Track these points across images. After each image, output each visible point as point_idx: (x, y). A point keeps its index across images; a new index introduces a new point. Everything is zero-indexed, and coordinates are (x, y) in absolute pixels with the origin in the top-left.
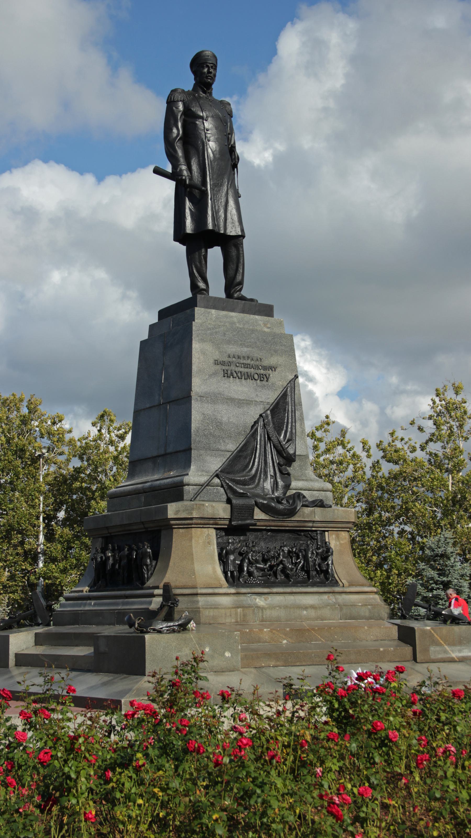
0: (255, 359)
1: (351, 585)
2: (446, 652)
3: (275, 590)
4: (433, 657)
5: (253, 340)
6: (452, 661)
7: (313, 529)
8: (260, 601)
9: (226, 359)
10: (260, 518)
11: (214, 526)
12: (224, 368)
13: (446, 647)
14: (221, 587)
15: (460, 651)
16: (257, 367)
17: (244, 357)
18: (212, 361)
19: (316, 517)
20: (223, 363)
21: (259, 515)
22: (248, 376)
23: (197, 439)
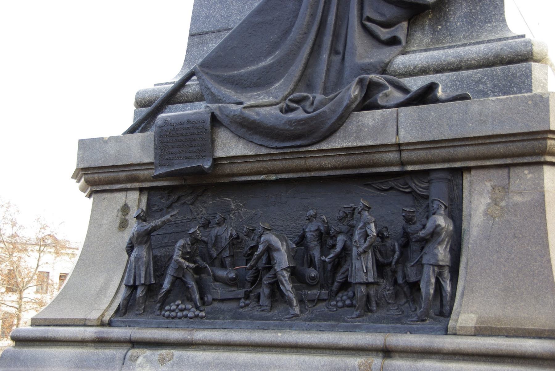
3: (201, 335)
7: (410, 168)
10: (232, 154)
11: (137, 185)
19: (402, 132)
23: (203, 14)
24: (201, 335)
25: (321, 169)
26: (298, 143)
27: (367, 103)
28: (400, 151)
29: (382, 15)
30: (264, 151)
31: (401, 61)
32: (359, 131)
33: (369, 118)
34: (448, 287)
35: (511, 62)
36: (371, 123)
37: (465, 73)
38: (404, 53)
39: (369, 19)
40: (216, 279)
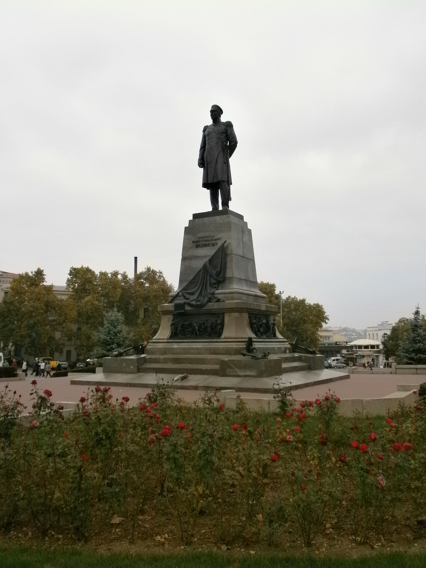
1: (225, 338)
2: (236, 372)
3: (184, 341)
4: (228, 374)
6: (239, 376)
8: (175, 346)
9: (197, 240)
12: (196, 244)
13: (236, 370)
14: (164, 339)
15: (245, 372)
16: (212, 240)
17: (206, 237)
18: (192, 242)
20: (197, 242)
21: (187, 308)
24: (184, 341)
27: (210, 301)
31: (217, 292)
33: (210, 304)
34: (221, 332)
35: (233, 293)
37: (226, 295)
38: (217, 290)
40: (187, 331)
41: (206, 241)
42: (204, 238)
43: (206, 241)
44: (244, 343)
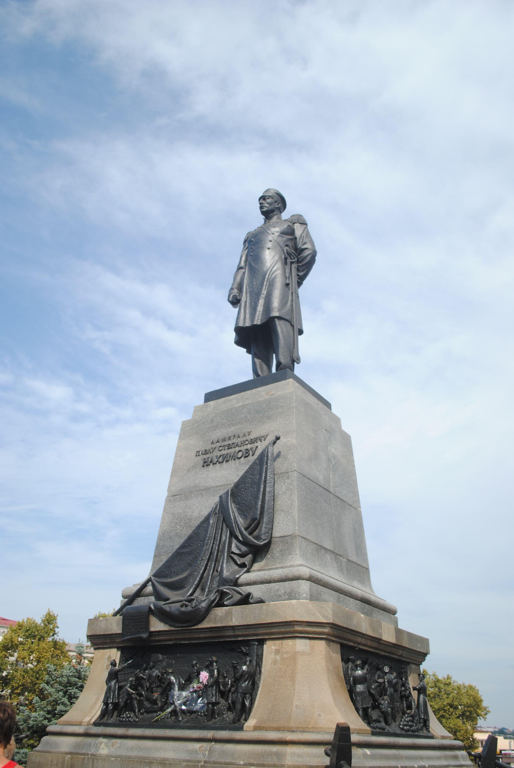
0: (241, 436)
5: (243, 415)
9: (209, 447)
11: (115, 645)
12: (205, 456)
16: (243, 443)
17: (229, 438)
18: (194, 453)
19: (234, 619)
20: (206, 452)
21: (157, 625)
22: (230, 457)
23: (161, 544)
25: (199, 638)
26: (188, 624)
28: (234, 630)
29: (240, 550)
30: (173, 629)
32: (215, 619)
33: (220, 611)
35: (292, 579)
36: (220, 614)
38: (248, 571)
39: (233, 553)
41: (229, 447)
42: (224, 440)
43: (229, 447)
44: (321, 750)
